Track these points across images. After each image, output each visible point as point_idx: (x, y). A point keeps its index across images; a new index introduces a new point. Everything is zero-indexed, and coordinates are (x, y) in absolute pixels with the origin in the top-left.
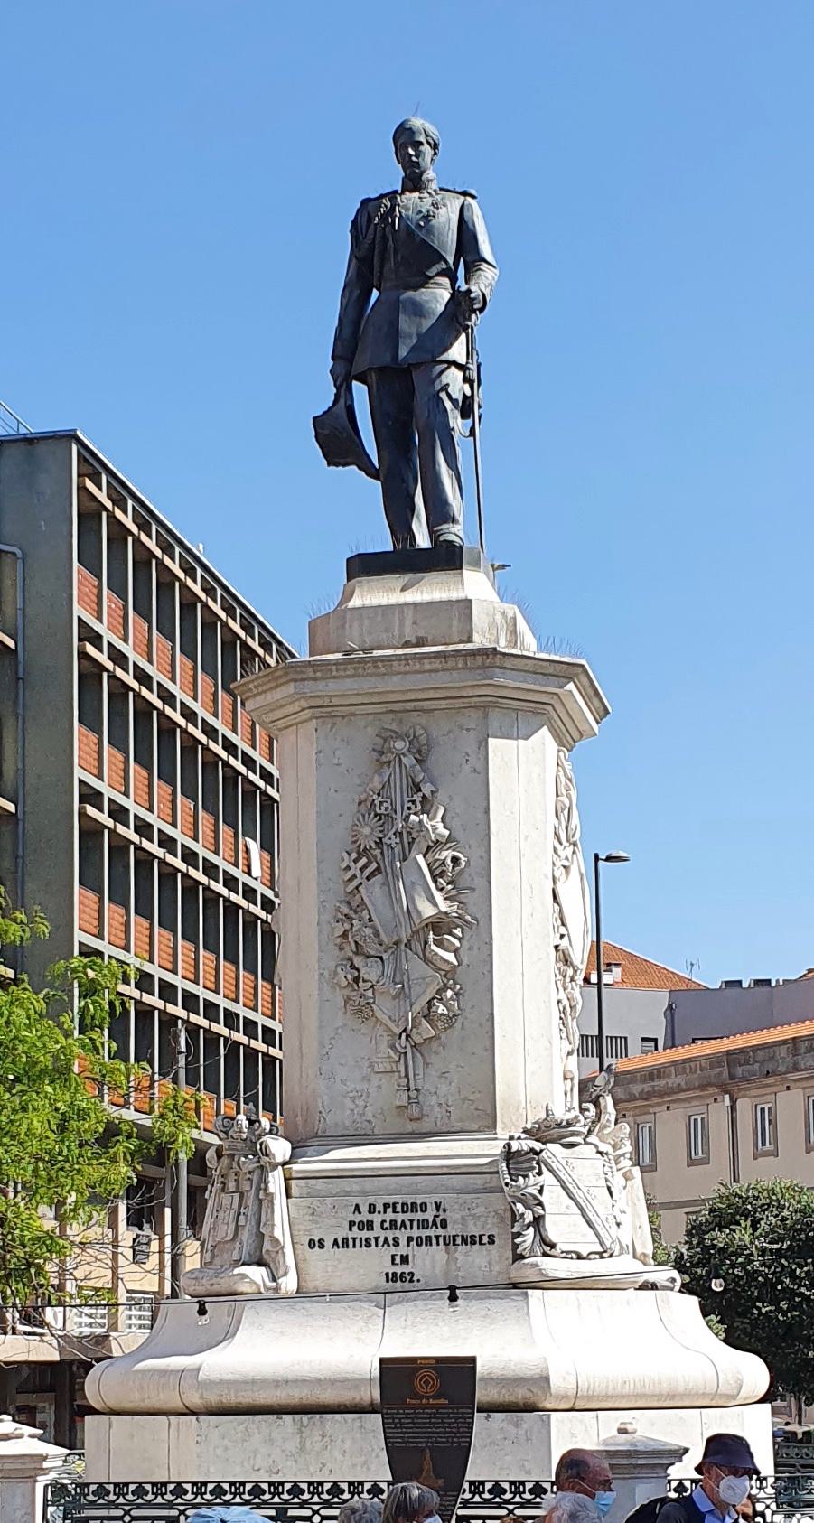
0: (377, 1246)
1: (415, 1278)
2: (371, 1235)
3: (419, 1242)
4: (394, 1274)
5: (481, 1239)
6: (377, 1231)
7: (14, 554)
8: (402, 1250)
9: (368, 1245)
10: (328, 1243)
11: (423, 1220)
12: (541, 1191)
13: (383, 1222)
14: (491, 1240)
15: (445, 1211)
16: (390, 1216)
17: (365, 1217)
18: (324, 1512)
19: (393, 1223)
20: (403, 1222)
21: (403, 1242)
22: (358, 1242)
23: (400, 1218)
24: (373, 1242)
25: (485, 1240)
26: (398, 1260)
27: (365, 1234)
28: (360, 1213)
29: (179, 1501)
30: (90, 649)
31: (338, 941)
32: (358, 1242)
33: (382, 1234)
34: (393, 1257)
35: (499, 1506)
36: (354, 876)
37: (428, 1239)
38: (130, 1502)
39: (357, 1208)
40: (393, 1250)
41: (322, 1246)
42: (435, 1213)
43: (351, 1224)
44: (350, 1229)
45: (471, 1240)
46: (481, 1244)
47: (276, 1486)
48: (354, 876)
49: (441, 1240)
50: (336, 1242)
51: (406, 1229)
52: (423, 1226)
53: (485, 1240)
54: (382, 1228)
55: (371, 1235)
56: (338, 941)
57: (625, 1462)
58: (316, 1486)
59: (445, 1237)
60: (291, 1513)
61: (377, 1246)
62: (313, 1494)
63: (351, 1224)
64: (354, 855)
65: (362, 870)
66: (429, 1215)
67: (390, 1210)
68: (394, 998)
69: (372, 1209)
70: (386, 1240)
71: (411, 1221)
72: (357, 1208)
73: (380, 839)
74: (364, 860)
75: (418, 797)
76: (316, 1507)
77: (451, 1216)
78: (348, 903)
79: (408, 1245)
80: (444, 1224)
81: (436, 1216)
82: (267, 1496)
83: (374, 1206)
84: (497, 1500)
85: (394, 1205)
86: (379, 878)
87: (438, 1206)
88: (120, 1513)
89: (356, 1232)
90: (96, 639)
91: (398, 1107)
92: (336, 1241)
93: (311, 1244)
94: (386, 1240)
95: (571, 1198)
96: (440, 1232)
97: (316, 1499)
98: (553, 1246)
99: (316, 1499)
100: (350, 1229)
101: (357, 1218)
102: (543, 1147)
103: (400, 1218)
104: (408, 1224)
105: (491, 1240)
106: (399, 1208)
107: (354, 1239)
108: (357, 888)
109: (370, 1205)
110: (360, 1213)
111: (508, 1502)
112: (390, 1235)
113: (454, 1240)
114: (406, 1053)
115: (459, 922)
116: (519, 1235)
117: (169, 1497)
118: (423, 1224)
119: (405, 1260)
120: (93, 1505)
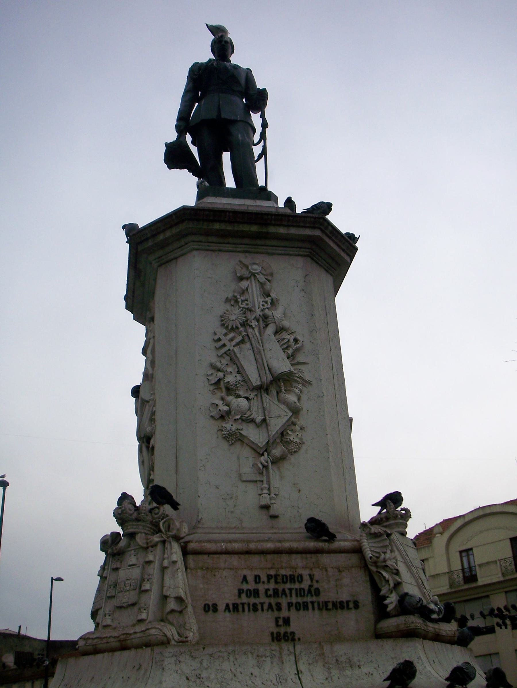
0: (263, 610)
1: (296, 637)
2: (257, 601)
3: (298, 607)
4: (279, 634)
6: (262, 598)
8: (285, 613)
10: (221, 607)
11: (300, 589)
14: (356, 605)
16: (272, 586)
17: (251, 586)
21: (284, 605)
22: (246, 607)
23: (281, 587)
24: (259, 607)
25: (351, 605)
26: (281, 622)
27: (252, 600)
28: (247, 582)
32: (246, 607)
33: (267, 601)
34: (277, 620)
36: (224, 345)
39: (245, 579)
40: (276, 614)
42: (309, 582)
45: (341, 606)
46: (348, 608)
48: (224, 345)
49: (316, 605)
51: (286, 596)
52: (300, 594)
53: (351, 605)
55: (257, 601)
59: (319, 603)
61: (263, 610)
63: (240, 592)
67: (272, 581)
69: (257, 579)
72: (245, 579)
74: (231, 335)
75: (268, 300)
77: (323, 586)
79: (289, 610)
80: (317, 592)
81: (311, 586)
83: (259, 576)
85: (276, 576)
87: (311, 577)
89: (244, 599)
92: (227, 605)
93: (207, 608)
94: (270, 606)
96: (314, 599)
101: (245, 587)
103: (281, 587)
107: (249, 604)
109: (256, 576)
110: (247, 582)
112: (273, 601)
118: (300, 592)
119: (287, 621)
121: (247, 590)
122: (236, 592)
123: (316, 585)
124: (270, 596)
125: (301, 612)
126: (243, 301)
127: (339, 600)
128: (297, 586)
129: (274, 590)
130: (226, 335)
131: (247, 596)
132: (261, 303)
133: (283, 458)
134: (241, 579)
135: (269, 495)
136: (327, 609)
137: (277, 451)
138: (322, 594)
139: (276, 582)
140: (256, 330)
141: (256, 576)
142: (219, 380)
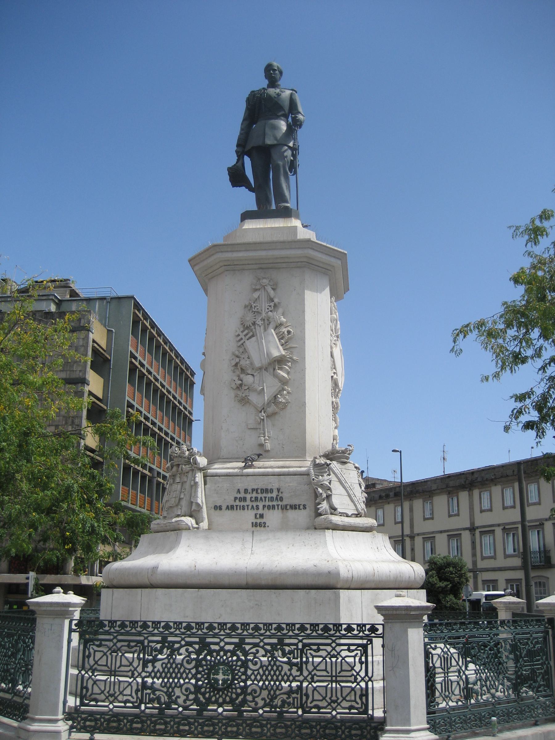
0: (248, 509)
1: (266, 525)
2: (245, 504)
3: (269, 507)
5: (299, 507)
6: (248, 502)
7: (112, 331)
8: (260, 511)
10: (224, 507)
12: (330, 483)
13: (251, 498)
14: (305, 507)
15: (282, 493)
16: (254, 495)
17: (242, 495)
18: (227, 640)
19: (256, 499)
20: (261, 498)
21: (261, 507)
22: (238, 507)
23: (259, 496)
24: (246, 508)
25: (301, 507)
26: (258, 516)
27: (242, 504)
28: (240, 493)
29: (145, 631)
30: (133, 360)
31: (233, 368)
32: (238, 507)
33: (251, 504)
34: (256, 515)
35: (327, 638)
36: (242, 339)
37: (273, 507)
38: (117, 632)
39: (239, 491)
40: (255, 511)
42: (277, 493)
44: (235, 501)
45: (294, 507)
46: (299, 509)
47: (199, 625)
48: (242, 339)
49: (280, 507)
53: (301, 507)
55: (245, 504)
58: (222, 625)
59: (281, 505)
60: (208, 640)
61: (248, 509)
63: (236, 499)
64: (242, 329)
65: (245, 336)
66: (274, 495)
67: (254, 492)
70: (253, 506)
71: (265, 497)
72: (239, 491)
73: (254, 322)
74: (246, 332)
75: (272, 304)
76: (222, 637)
77: (285, 495)
79: (263, 509)
80: (281, 499)
81: (277, 495)
82: (194, 630)
83: (247, 490)
84: (326, 634)
86: (254, 339)
87: (278, 490)
88: (112, 637)
89: (237, 503)
90: (136, 358)
92: (228, 506)
94: (253, 506)
95: (344, 488)
96: (280, 503)
97: (222, 633)
98: (335, 509)
99: (222, 633)
100: (235, 501)
101: (239, 496)
102: (331, 462)
103: (259, 496)
104: (263, 499)
105: (305, 507)
106: (259, 491)
108: (242, 344)
110: (240, 493)
111: (333, 635)
112: (255, 504)
113: (286, 507)
115: (289, 359)
116: (319, 504)
117: (139, 629)
118: (271, 499)
119: (262, 516)
121: (240, 498)
122: (233, 499)
123: (280, 495)
124: (253, 501)
125: (271, 511)
126: (255, 306)
127: (294, 504)
129: (255, 497)
130: (242, 332)
133: (274, 414)
134: (236, 491)
135: (264, 437)
136: (286, 509)
137: (270, 410)
138: (284, 500)
139: (257, 493)
140: (262, 328)
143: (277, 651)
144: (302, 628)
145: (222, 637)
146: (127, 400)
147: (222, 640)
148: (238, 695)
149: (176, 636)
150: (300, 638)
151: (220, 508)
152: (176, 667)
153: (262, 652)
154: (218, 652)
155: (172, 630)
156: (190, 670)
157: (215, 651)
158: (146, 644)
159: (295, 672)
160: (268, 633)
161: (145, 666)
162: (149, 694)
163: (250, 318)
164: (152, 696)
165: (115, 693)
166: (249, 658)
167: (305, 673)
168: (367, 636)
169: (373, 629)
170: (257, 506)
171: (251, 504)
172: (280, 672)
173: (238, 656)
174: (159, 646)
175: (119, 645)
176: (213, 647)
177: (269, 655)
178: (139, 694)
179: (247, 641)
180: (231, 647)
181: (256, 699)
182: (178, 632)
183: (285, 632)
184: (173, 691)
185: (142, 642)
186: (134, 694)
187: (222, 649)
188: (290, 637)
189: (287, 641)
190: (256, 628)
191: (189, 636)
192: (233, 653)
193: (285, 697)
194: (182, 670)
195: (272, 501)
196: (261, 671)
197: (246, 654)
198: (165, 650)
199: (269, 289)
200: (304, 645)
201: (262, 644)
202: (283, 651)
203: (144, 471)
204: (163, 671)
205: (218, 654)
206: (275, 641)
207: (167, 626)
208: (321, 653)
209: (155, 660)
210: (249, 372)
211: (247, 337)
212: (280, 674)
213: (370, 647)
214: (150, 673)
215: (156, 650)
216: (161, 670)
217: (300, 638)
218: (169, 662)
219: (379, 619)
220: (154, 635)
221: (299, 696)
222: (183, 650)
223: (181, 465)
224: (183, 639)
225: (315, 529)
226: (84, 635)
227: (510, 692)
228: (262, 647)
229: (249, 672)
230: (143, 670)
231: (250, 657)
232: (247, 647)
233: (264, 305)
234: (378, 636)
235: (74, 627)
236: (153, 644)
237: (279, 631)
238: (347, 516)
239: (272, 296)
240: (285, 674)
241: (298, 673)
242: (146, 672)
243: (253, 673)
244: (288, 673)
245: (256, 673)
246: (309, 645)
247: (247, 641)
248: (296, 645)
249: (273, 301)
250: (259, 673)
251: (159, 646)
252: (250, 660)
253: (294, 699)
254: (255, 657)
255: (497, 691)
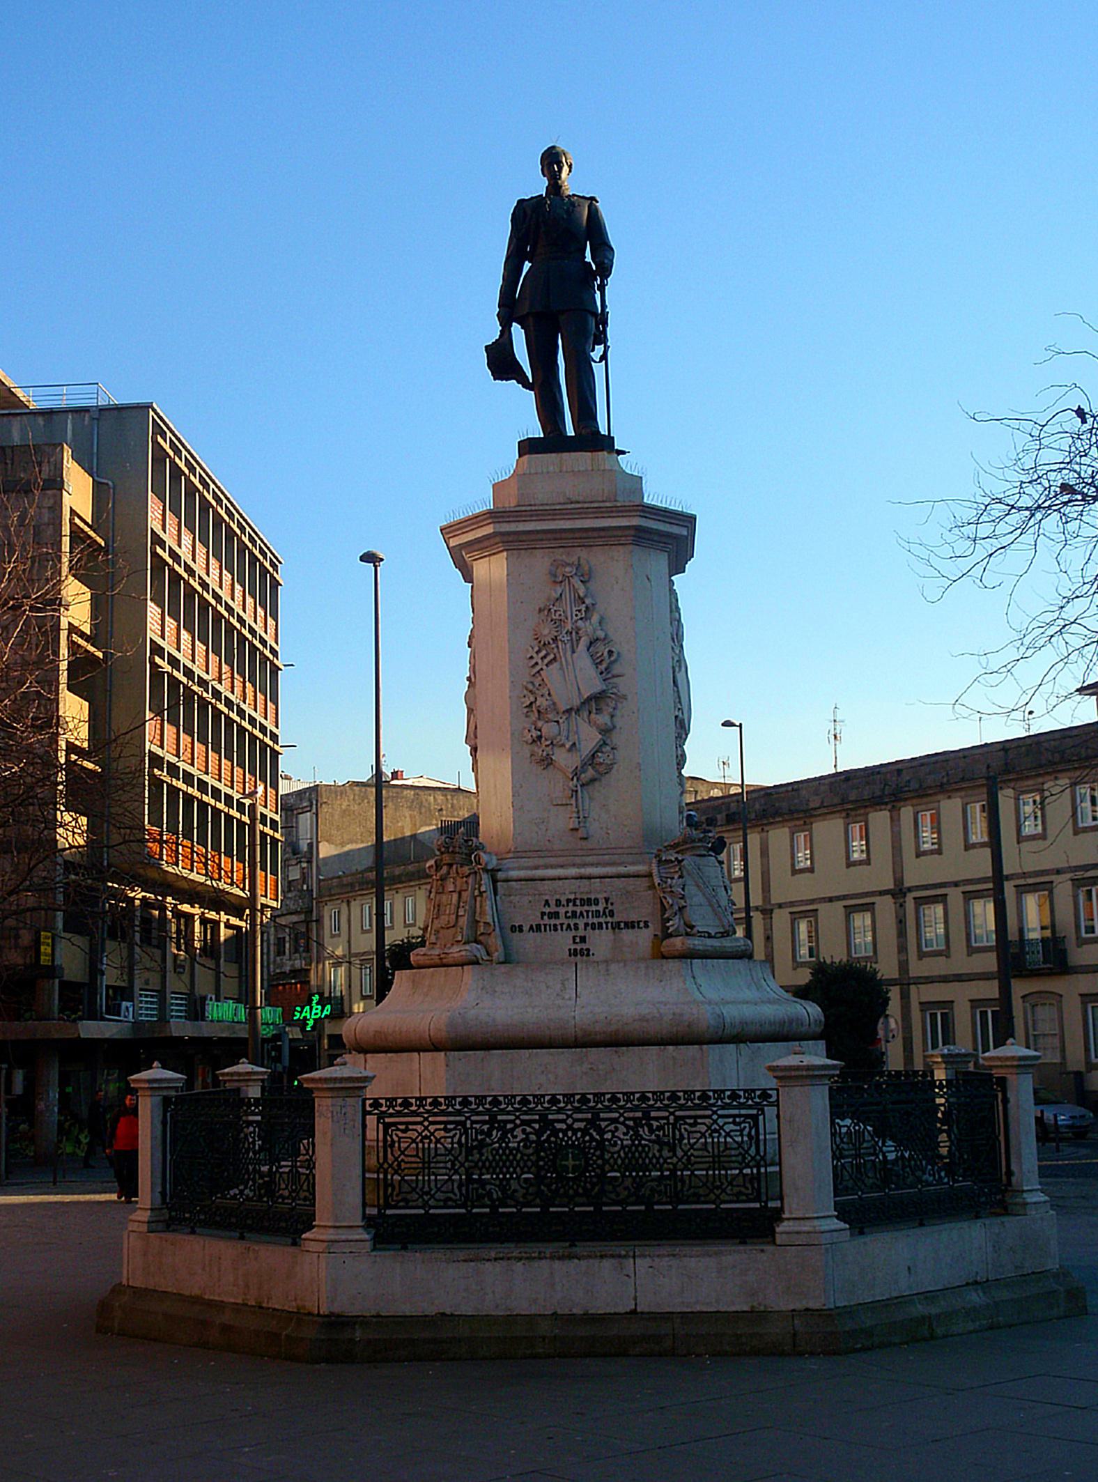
2: (557, 922)
4: (575, 950)
6: (562, 920)
7: (107, 484)
8: (581, 932)
9: (556, 930)
10: (526, 928)
12: (683, 889)
13: (567, 912)
14: (646, 926)
15: (612, 904)
16: (571, 908)
17: (553, 909)
18: (575, 1116)
19: (574, 913)
20: (581, 913)
21: (581, 926)
24: (559, 927)
25: (642, 925)
26: (578, 940)
27: (553, 922)
30: (159, 550)
31: (525, 710)
33: (566, 922)
34: (574, 938)
35: (705, 1108)
36: (537, 663)
37: (600, 924)
38: (428, 1112)
39: (547, 903)
40: (573, 933)
41: (521, 930)
43: (543, 914)
44: (542, 918)
45: (630, 925)
46: (639, 927)
47: (539, 1098)
48: (537, 663)
50: (531, 927)
53: (642, 925)
54: (566, 917)
55: (557, 922)
56: (525, 710)
57: (804, 1073)
60: (550, 1117)
62: (508, 1105)
63: (543, 914)
64: (536, 649)
65: (542, 658)
66: (600, 908)
67: (571, 904)
68: (570, 750)
69: (558, 903)
70: (569, 926)
72: (547, 903)
74: (544, 653)
76: (570, 1113)
78: (532, 683)
79: (585, 929)
80: (612, 914)
86: (555, 665)
87: (607, 900)
90: (162, 543)
91: (572, 830)
93: (513, 929)
94: (569, 926)
96: (609, 919)
98: (692, 927)
100: (542, 918)
101: (547, 910)
104: (585, 914)
105: (646, 926)
106: (578, 902)
107: (545, 925)
108: (538, 672)
109: (557, 900)
111: (713, 1105)
112: (572, 922)
114: (577, 791)
116: (669, 920)
119: (583, 939)
120: (399, 1114)
123: (610, 908)
125: (597, 931)
128: (594, 908)
129: (573, 912)
130: (537, 652)
131: (549, 918)
132: (574, 613)
133: (593, 780)
139: (575, 905)
140: (568, 646)
141: (557, 900)
142: (531, 703)
143: (642, 1127)
144: (674, 1096)
145: (570, 1113)
146: (151, 639)
147: (568, 1116)
148: (594, 1185)
149: (509, 1113)
150: (671, 1110)
151: (521, 929)
152: (511, 1153)
153: (622, 1129)
154: (565, 1132)
155: (503, 1106)
156: (528, 1156)
157: (561, 1130)
158: (468, 1126)
159: (666, 1153)
160: (629, 1105)
161: (469, 1151)
162: (477, 1189)
163: (547, 632)
164: (480, 1191)
165: (431, 1190)
166: (605, 1137)
167: (680, 1153)
168: (757, 1104)
169: (765, 1095)
170: (576, 925)
171: (566, 922)
172: (647, 1154)
173: (591, 1135)
174: (485, 1127)
175: (432, 1128)
176: (558, 1126)
177: (631, 1133)
178: (464, 1189)
179: (602, 1115)
180: (582, 1125)
181: (618, 1189)
182: (510, 1108)
183: (652, 1102)
184: (508, 1184)
185: (463, 1124)
186: (456, 1191)
187: (570, 1127)
188: (659, 1109)
189: (653, 1114)
190: (614, 1099)
191: (526, 1113)
192: (585, 1132)
193: (654, 1184)
194: (519, 1156)
195: (598, 917)
196: (622, 1154)
197: (601, 1132)
198: (494, 1133)
199: (576, 582)
200: (677, 1119)
201: (622, 1119)
202: (650, 1127)
203: (190, 790)
204: (494, 1159)
205: (565, 1134)
206: (639, 1114)
207: (495, 1102)
208: (699, 1128)
209: (482, 1144)
210: (550, 716)
211: (546, 661)
212: (647, 1156)
213: (761, 1118)
214: (476, 1163)
215: (482, 1132)
216: (491, 1158)
217: (671, 1110)
218: (500, 1147)
219: (773, 1083)
220: (478, 1114)
221: (672, 1183)
222: (518, 1132)
223: (454, 867)
224: (518, 1117)
225: (664, 957)
226: (383, 1118)
227: (943, 1174)
228: (623, 1123)
229: (607, 1156)
230: (467, 1160)
231: (608, 1136)
232: (603, 1124)
233: (568, 608)
234: (771, 1104)
235: (368, 1109)
236: (478, 1126)
237: (644, 1103)
238: (710, 936)
239: (582, 595)
240: (654, 1155)
241: (671, 1154)
242: (472, 1161)
243: (612, 1157)
244: (657, 1155)
245: (616, 1156)
246: (683, 1118)
247: (602, 1115)
248: (667, 1118)
249: (584, 603)
250: (619, 1156)
251: (485, 1127)
252: (607, 1140)
253: (666, 1186)
254: (613, 1136)
255: (924, 1173)
